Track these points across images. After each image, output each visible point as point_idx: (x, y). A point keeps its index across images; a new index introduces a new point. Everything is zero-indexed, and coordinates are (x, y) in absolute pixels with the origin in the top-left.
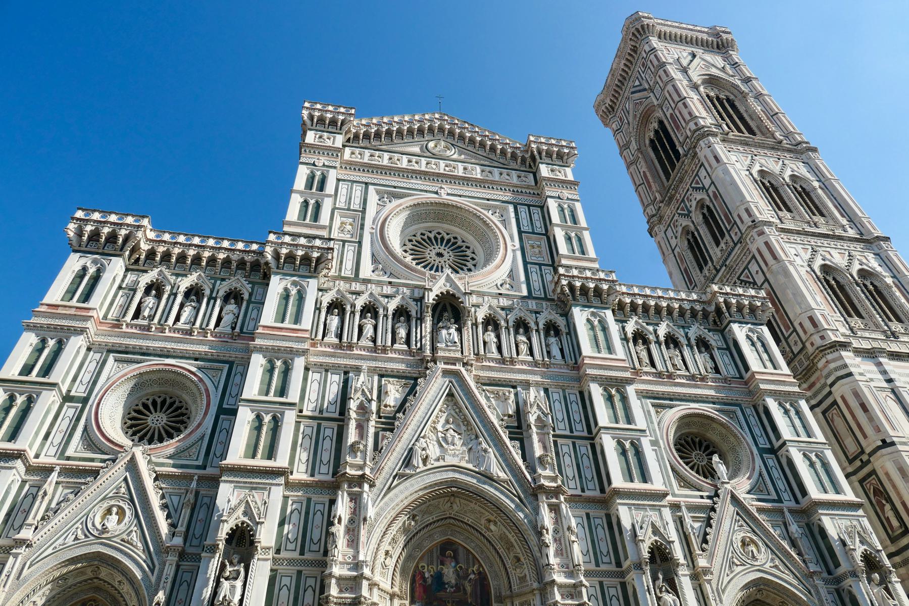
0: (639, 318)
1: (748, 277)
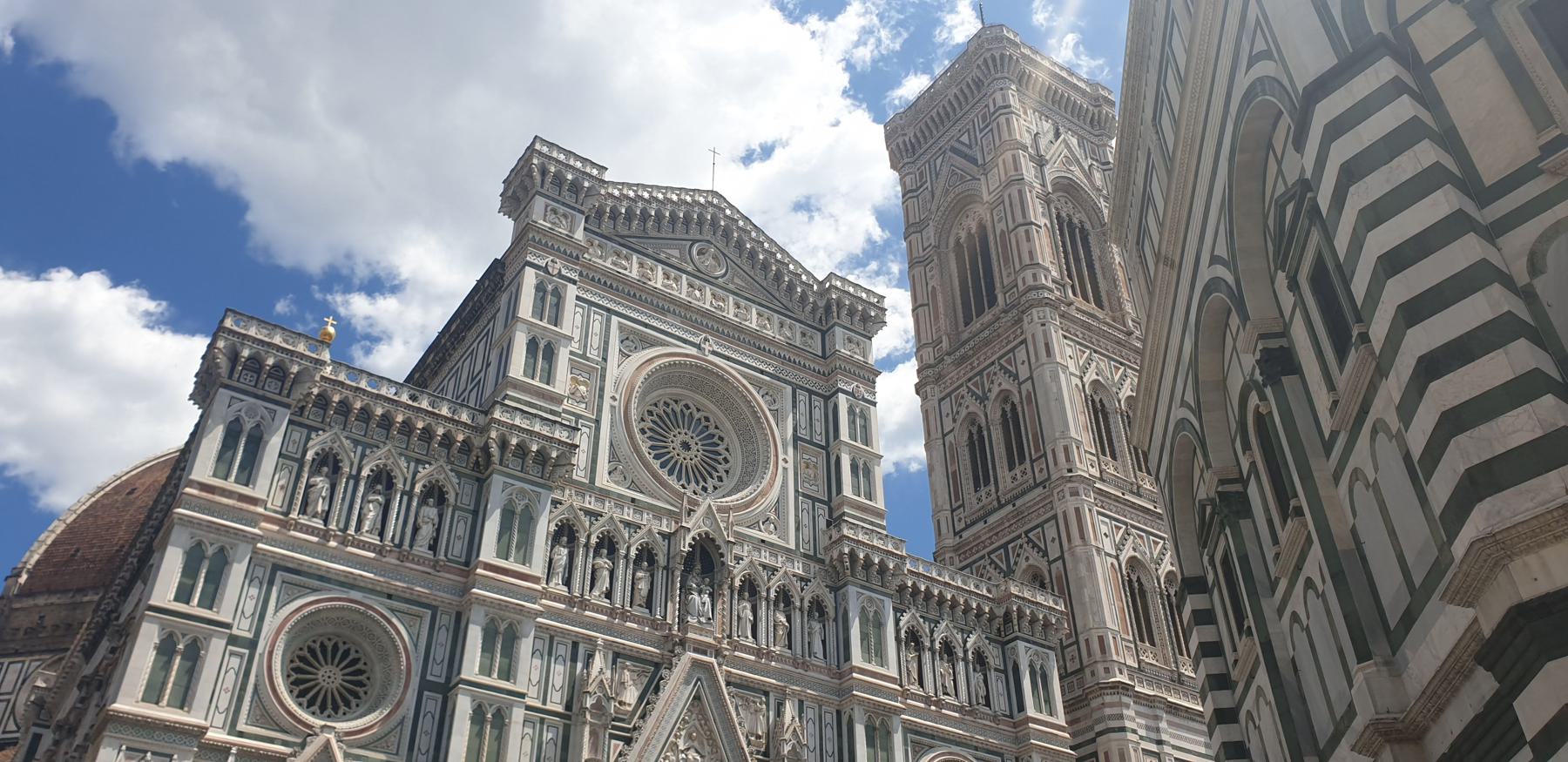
0: (917, 609)
1: (1039, 539)
